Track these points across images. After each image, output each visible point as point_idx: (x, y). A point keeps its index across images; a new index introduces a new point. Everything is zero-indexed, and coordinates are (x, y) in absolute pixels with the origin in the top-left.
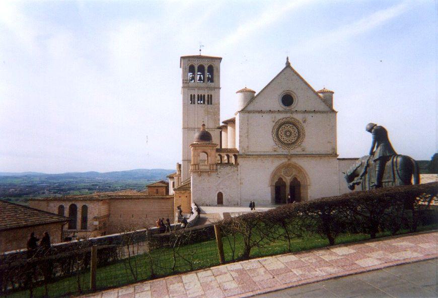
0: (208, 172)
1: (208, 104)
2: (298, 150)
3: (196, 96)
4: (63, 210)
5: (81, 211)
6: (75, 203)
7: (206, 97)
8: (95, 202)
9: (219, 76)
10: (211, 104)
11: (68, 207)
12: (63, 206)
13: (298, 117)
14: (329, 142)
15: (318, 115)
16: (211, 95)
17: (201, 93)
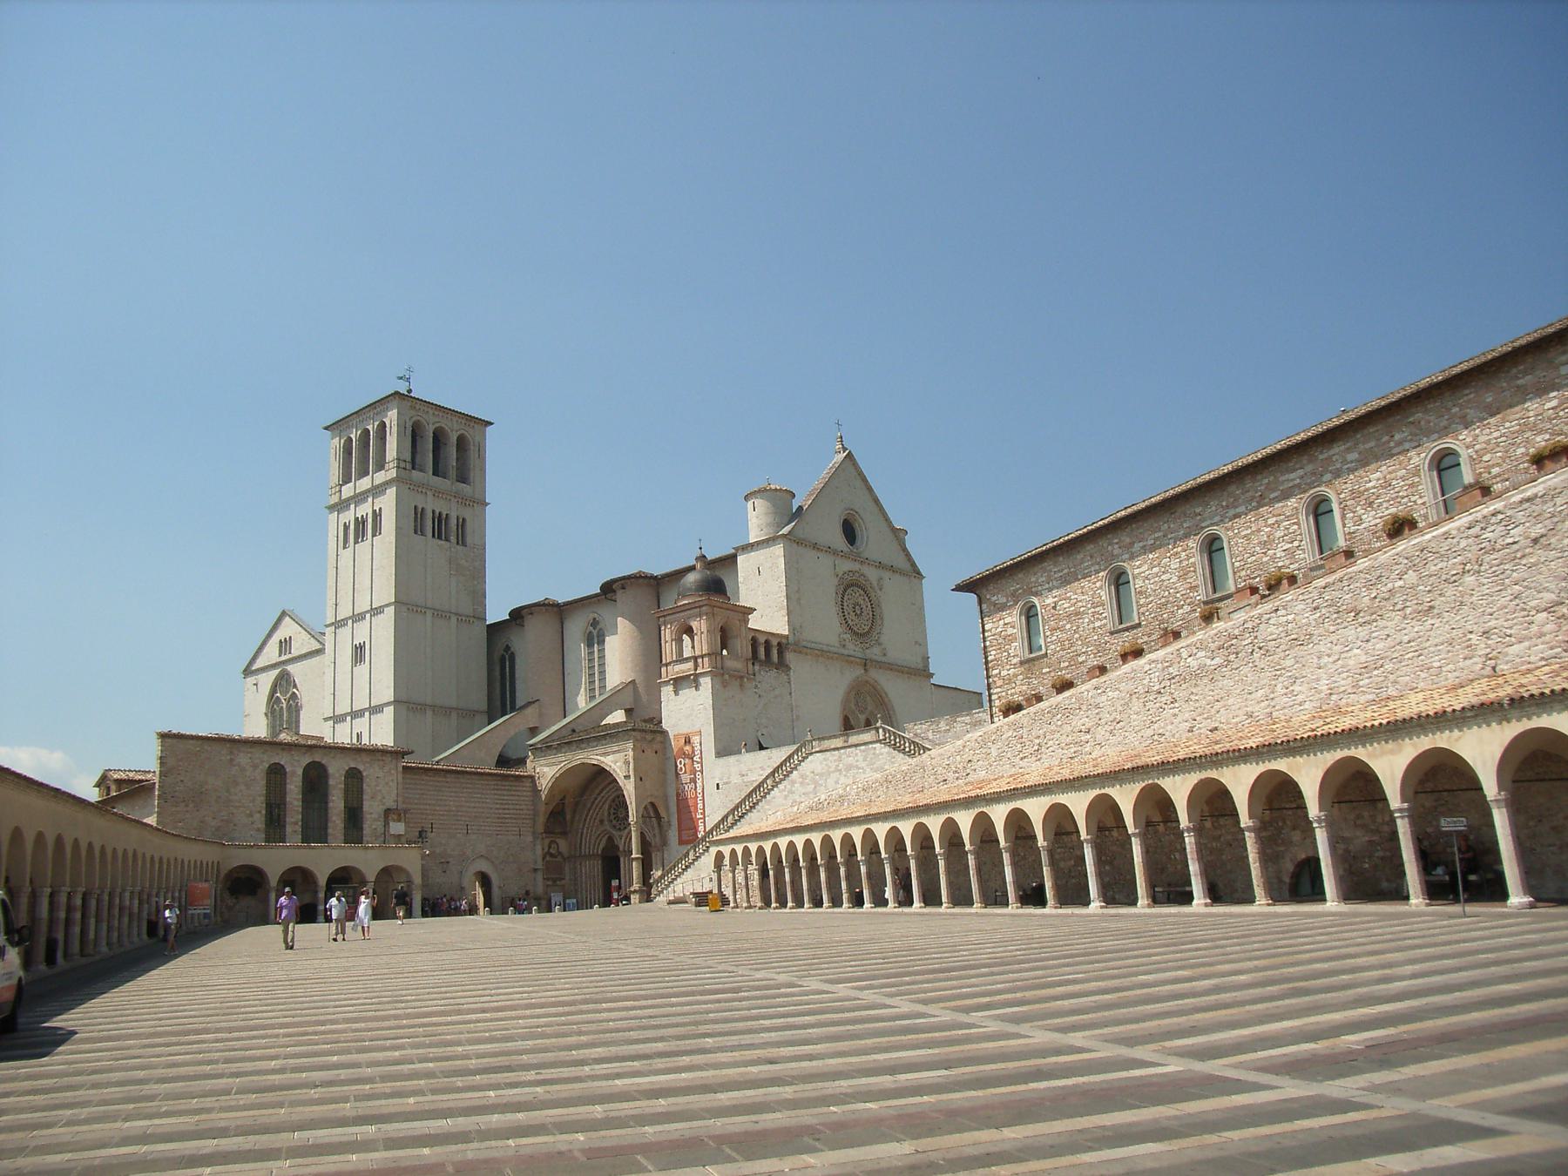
0: (742, 677)
1: (458, 543)
2: (874, 652)
3: (429, 515)
4: (283, 784)
5: (343, 786)
6: (323, 762)
7: (453, 522)
8: (388, 758)
9: (483, 470)
10: (464, 544)
11: (300, 772)
12: (283, 766)
13: (872, 574)
14: (916, 643)
15: (897, 576)
16: (464, 519)
17: (441, 507)
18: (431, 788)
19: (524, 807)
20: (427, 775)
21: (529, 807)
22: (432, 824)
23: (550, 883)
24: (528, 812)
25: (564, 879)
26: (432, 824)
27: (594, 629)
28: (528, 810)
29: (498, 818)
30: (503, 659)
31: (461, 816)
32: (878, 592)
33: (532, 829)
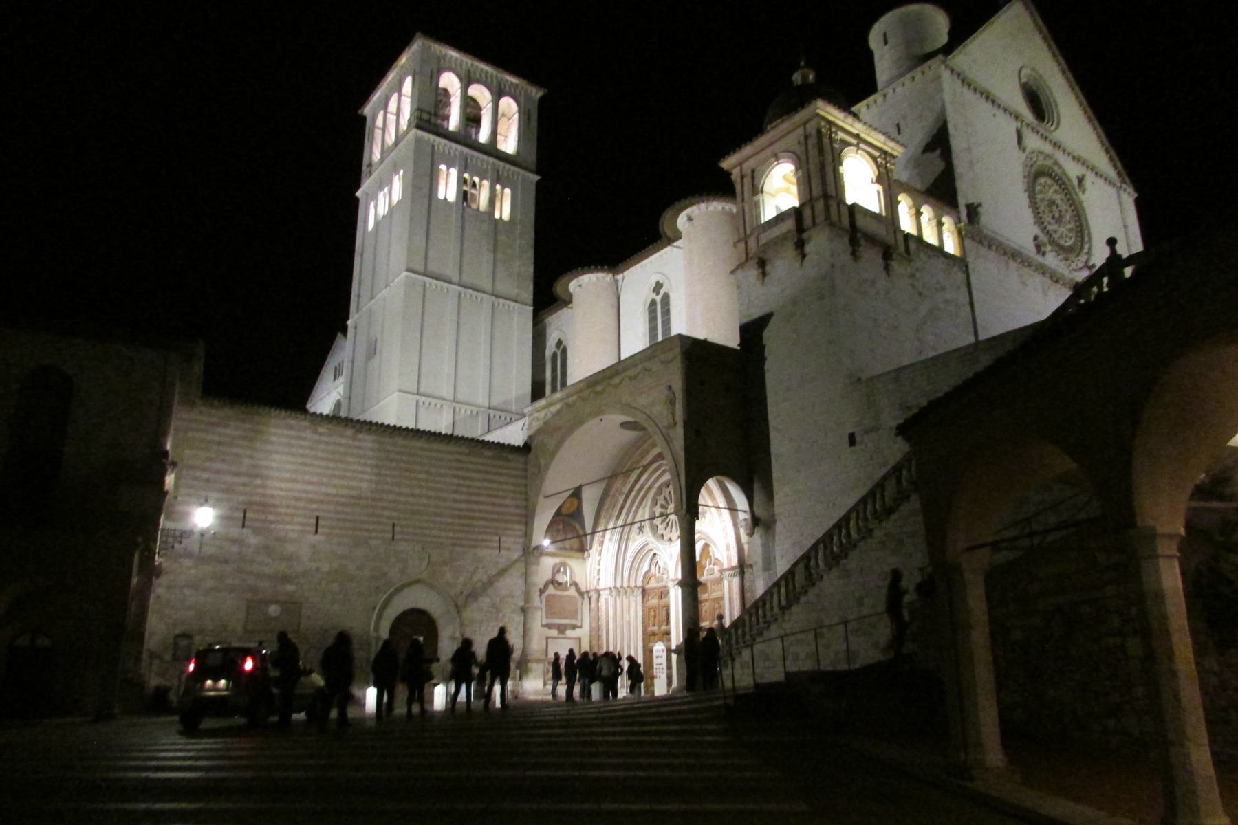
15: (1101, 182)
18: (320, 454)
19: (508, 502)
20: (316, 432)
21: (519, 503)
22: (317, 518)
23: (554, 633)
24: (518, 511)
25: (581, 627)
26: (317, 518)
27: (658, 294)
28: (517, 507)
29: (460, 517)
30: (555, 355)
31: (384, 508)
32: (1080, 194)
33: (521, 540)
